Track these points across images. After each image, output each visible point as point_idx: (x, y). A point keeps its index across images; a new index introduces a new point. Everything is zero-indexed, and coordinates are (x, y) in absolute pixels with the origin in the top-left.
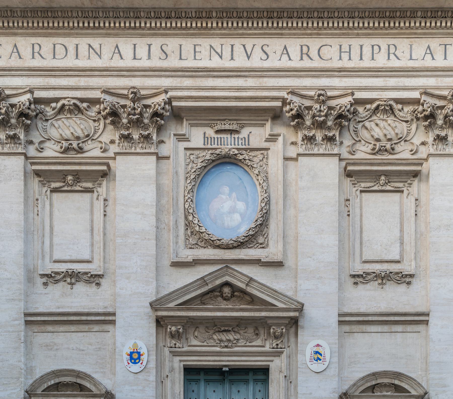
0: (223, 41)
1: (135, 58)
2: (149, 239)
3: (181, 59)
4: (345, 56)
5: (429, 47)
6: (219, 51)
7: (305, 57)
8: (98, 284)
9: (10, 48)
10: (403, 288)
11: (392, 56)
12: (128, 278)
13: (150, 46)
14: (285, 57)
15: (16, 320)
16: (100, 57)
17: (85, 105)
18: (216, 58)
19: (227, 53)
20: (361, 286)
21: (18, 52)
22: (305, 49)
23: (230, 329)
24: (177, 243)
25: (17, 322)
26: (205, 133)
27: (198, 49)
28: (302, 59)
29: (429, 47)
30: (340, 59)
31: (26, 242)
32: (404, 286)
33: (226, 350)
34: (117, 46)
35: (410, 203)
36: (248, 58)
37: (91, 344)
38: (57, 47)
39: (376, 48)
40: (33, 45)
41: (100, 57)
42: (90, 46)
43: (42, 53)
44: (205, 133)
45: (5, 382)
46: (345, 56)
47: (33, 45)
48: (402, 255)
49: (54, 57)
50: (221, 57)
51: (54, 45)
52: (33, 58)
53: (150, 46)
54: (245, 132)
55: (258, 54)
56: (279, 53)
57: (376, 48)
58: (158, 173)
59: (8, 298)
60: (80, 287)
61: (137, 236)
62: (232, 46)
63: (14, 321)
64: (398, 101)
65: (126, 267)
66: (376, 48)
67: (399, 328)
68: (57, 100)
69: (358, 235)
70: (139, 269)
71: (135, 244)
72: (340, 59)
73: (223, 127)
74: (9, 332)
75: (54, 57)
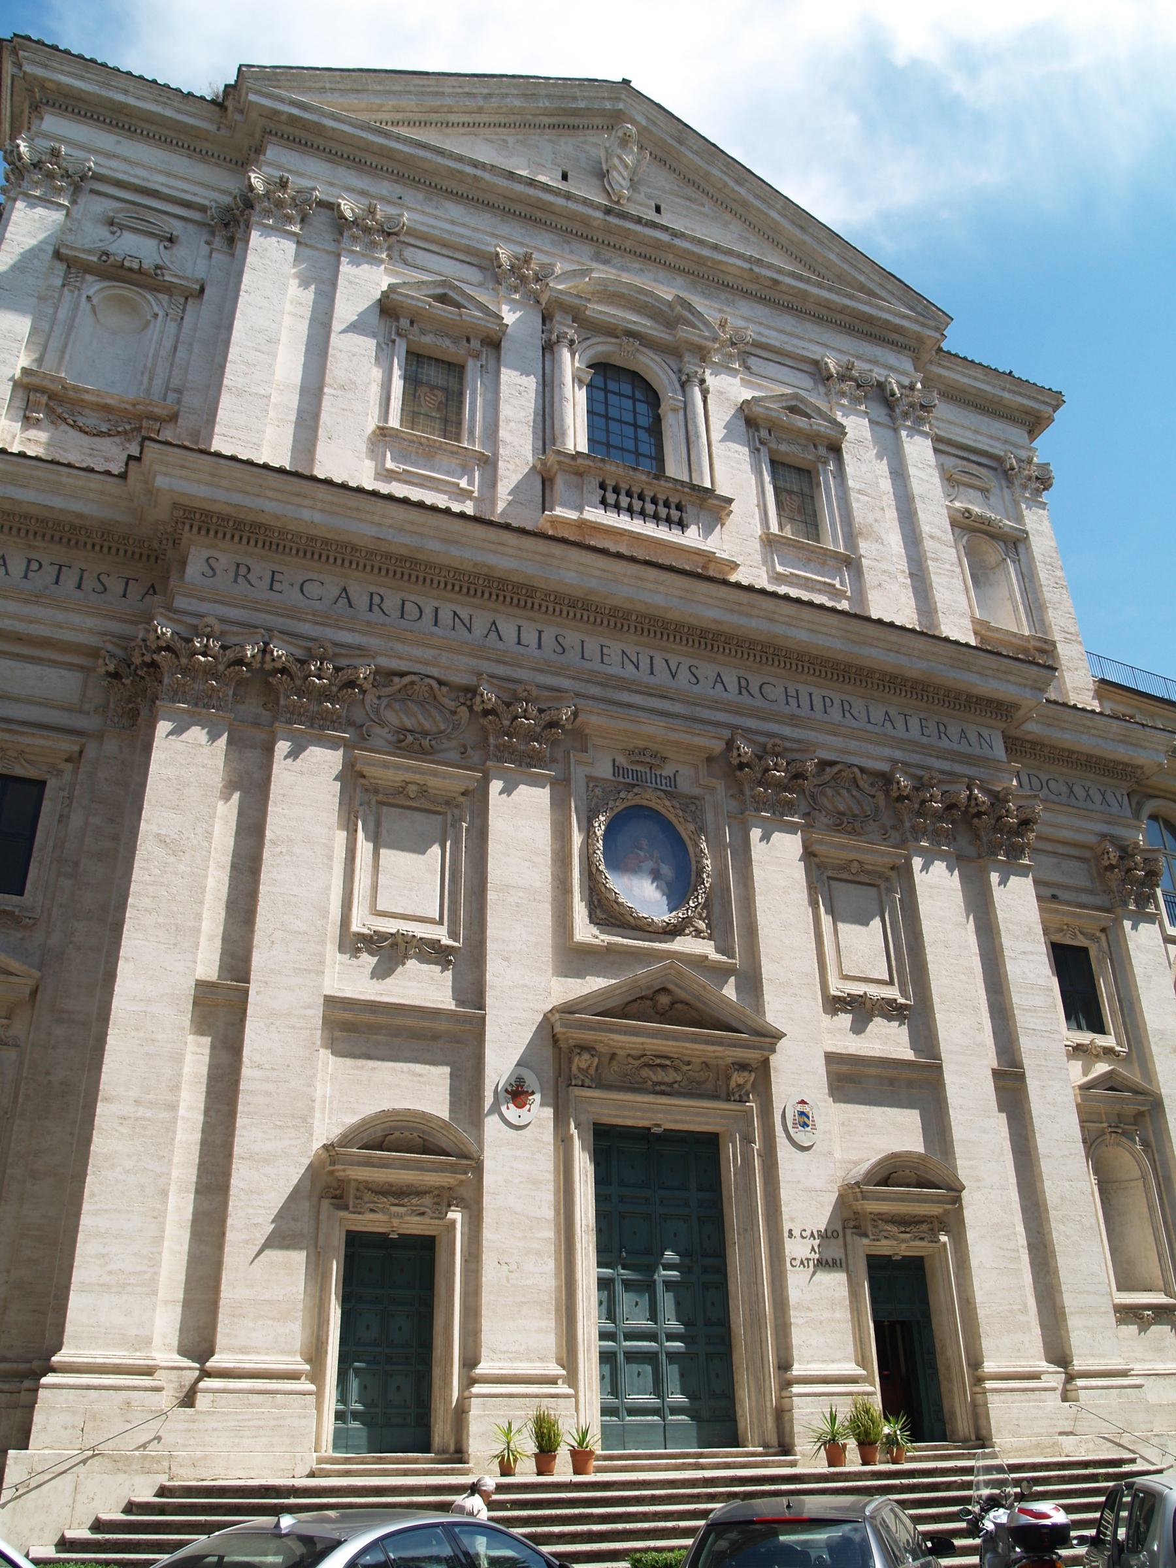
1: (519, 643)
2: (539, 901)
3: (583, 658)
4: (793, 701)
5: (887, 713)
6: (635, 660)
7: (744, 691)
9: (336, 591)
12: (506, 959)
13: (540, 632)
14: (719, 686)
15: (309, 1007)
16: (470, 631)
17: (444, 689)
18: (630, 668)
19: (645, 664)
21: (348, 598)
23: (668, 1062)
25: (310, 1012)
26: (614, 760)
27: (605, 650)
28: (740, 693)
29: (887, 713)
30: (787, 703)
34: (494, 623)
36: (673, 677)
38: (408, 605)
40: (372, 594)
41: (470, 631)
42: (455, 613)
43: (384, 606)
44: (614, 760)
45: (279, 1123)
46: (793, 701)
47: (372, 594)
49: (402, 617)
50: (637, 668)
51: (403, 602)
52: (371, 610)
53: (540, 632)
55: (684, 675)
56: (712, 678)
59: (297, 966)
61: (521, 894)
62: (651, 658)
63: (305, 1008)
65: (504, 941)
66: (827, 700)
68: (402, 674)
70: (524, 947)
71: (518, 905)
72: (787, 703)
74: (294, 1027)
75: (402, 617)
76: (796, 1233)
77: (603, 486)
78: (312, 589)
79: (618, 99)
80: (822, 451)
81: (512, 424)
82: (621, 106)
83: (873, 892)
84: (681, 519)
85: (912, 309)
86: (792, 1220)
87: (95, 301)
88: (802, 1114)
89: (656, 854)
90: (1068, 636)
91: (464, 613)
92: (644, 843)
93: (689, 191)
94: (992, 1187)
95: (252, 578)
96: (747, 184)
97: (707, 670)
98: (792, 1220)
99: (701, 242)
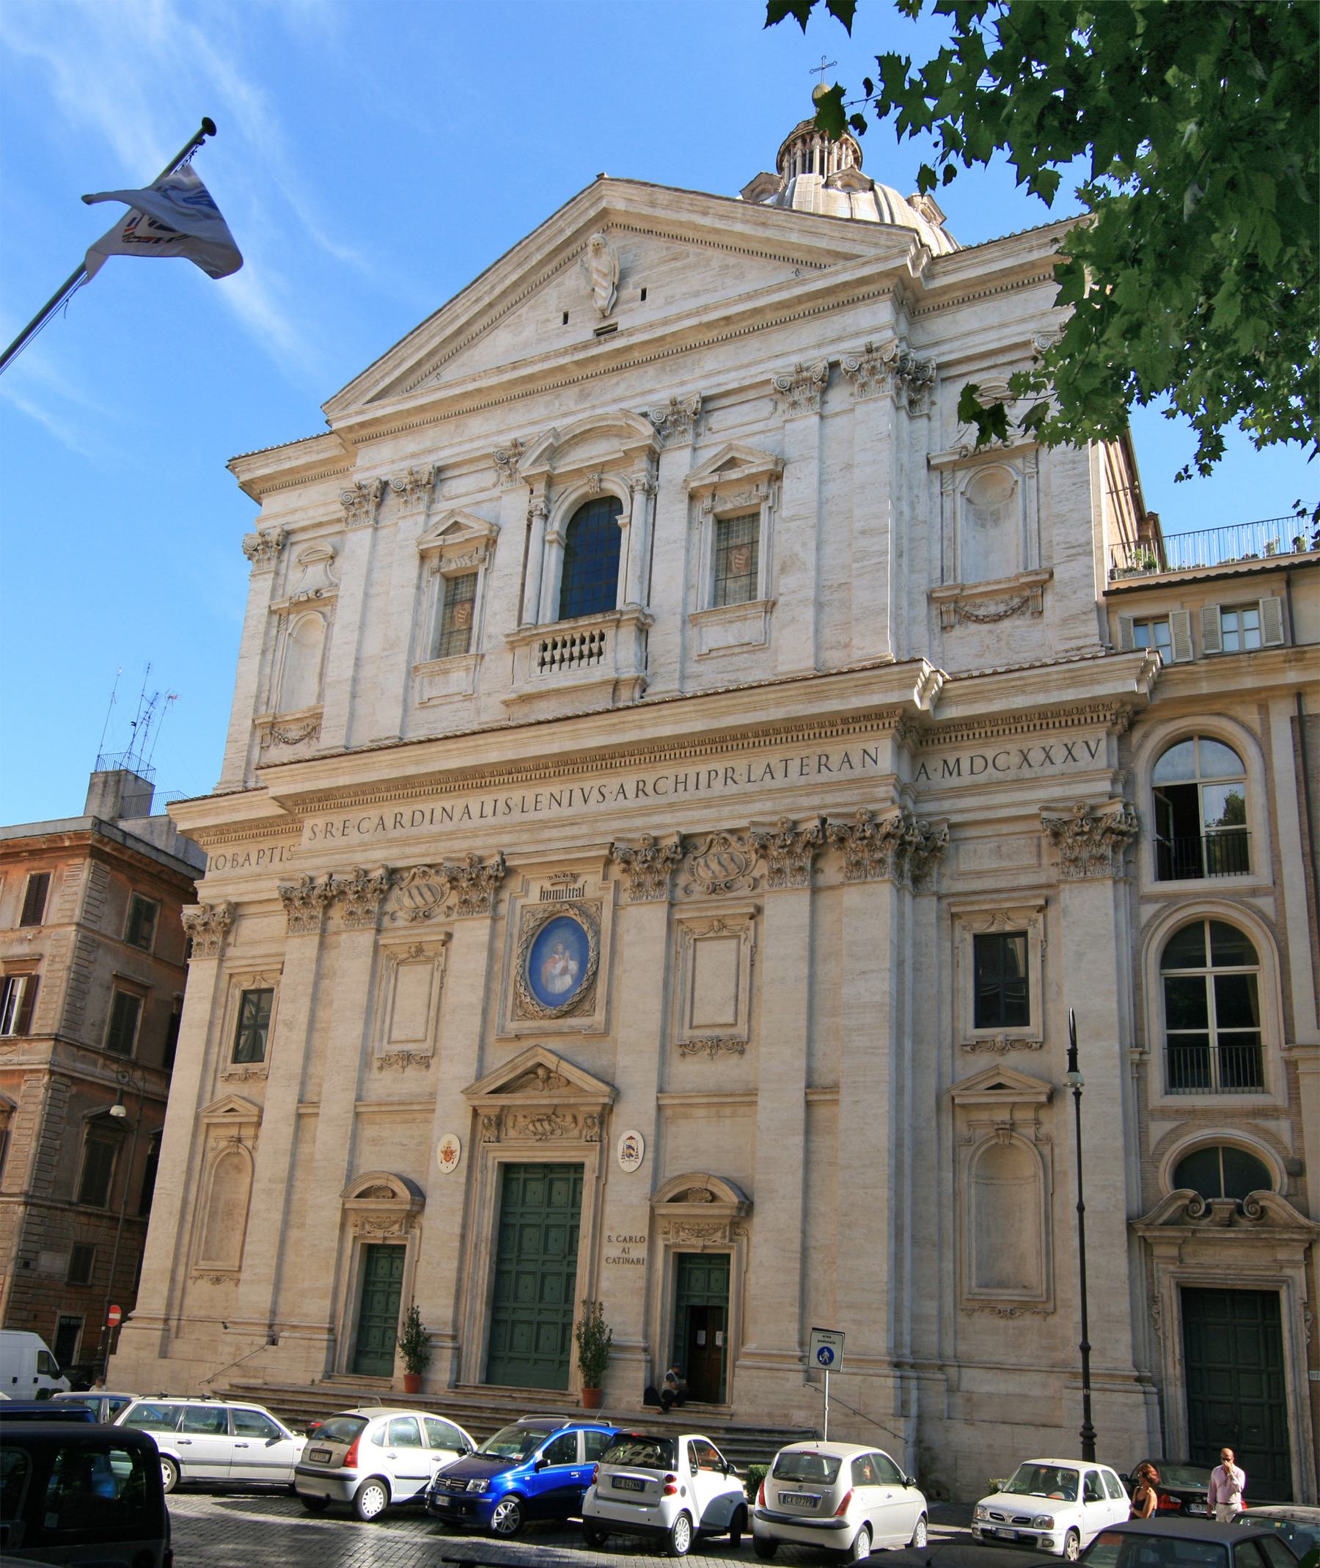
0: (562, 787)
4: (681, 787)
8: (428, 1067)
9: (376, 820)
10: (734, 1059)
11: (729, 781)
14: (621, 796)
19: (565, 801)
20: (688, 1059)
22: (641, 784)
24: (504, 1015)
31: (367, 1023)
32: (736, 1055)
33: (538, 1144)
35: (746, 950)
37: (412, 1137)
39: (713, 774)
46: (681, 787)
48: (736, 1020)
54: (579, 885)
56: (615, 793)
57: (713, 774)
58: (493, 935)
60: (411, 1071)
64: (731, 831)
67: (728, 1111)
69: (689, 995)
73: (558, 880)
76: (614, 1239)
77: (545, 648)
78: (364, 826)
79: (601, 198)
80: (763, 490)
81: (498, 617)
82: (604, 204)
83: (733, 943)
84: (600, 648)
85: (876, 245)
86: (612, 1229)
87: (295, 634)
88: (630, 1147)
89: (567, 954)
90: (1073, 551)
91: (449, 809)
92: (560, 947)
93: (679, 247)
94: (784, 1197)
95: (334, 831)
96: (711, 211)
97: (612, 783)
98: (612, 1229)
99: (651, 326)
